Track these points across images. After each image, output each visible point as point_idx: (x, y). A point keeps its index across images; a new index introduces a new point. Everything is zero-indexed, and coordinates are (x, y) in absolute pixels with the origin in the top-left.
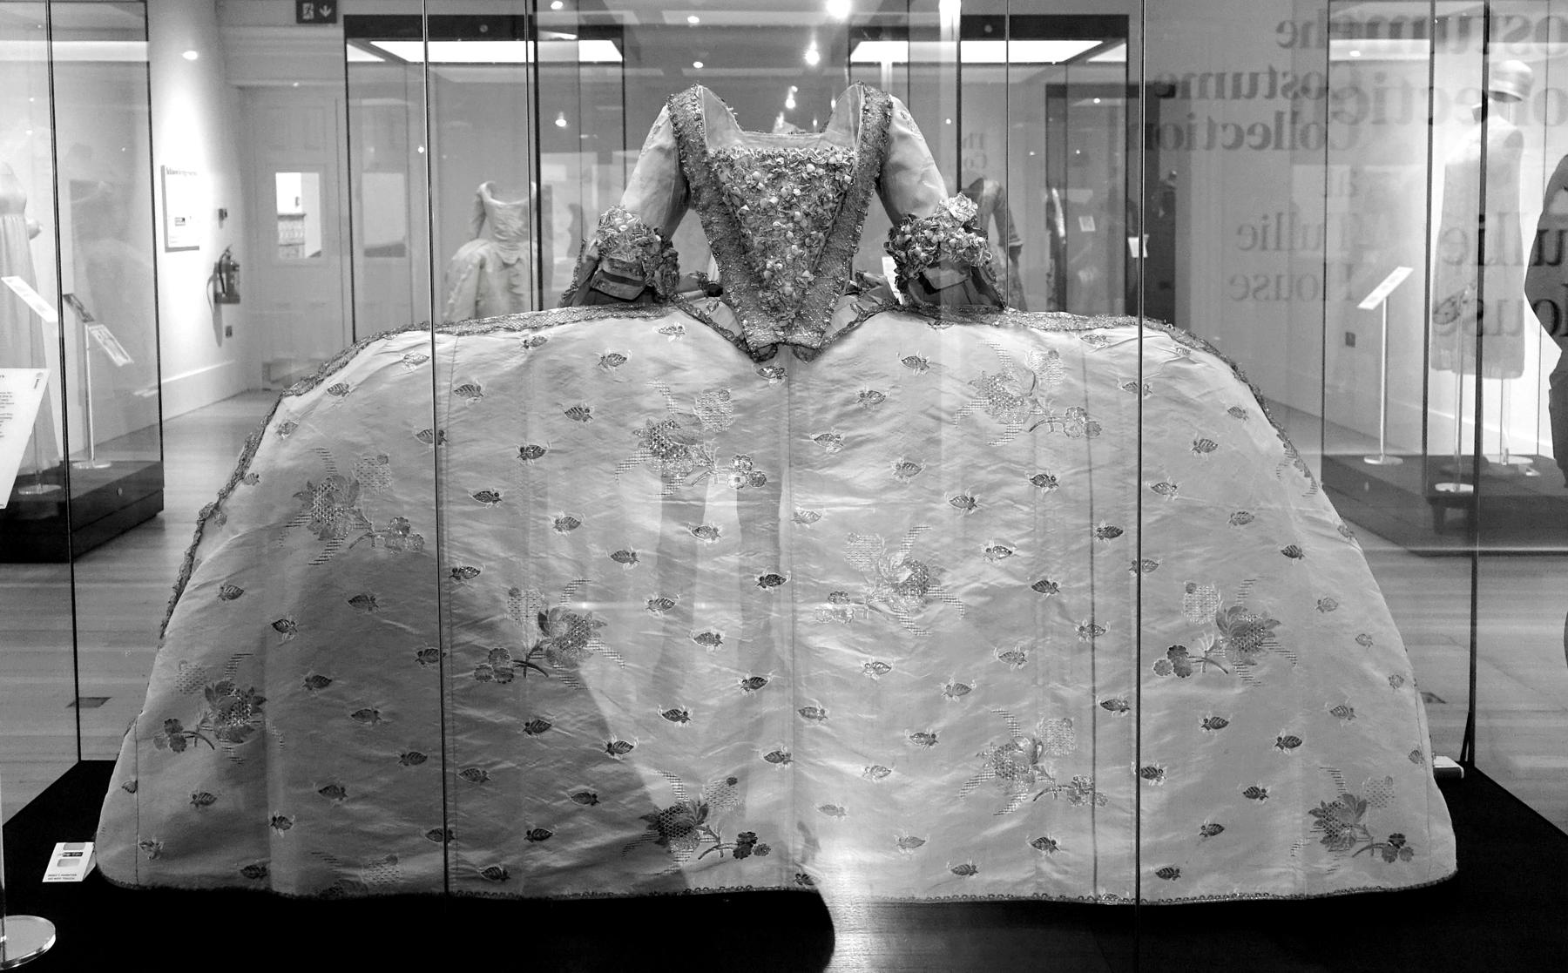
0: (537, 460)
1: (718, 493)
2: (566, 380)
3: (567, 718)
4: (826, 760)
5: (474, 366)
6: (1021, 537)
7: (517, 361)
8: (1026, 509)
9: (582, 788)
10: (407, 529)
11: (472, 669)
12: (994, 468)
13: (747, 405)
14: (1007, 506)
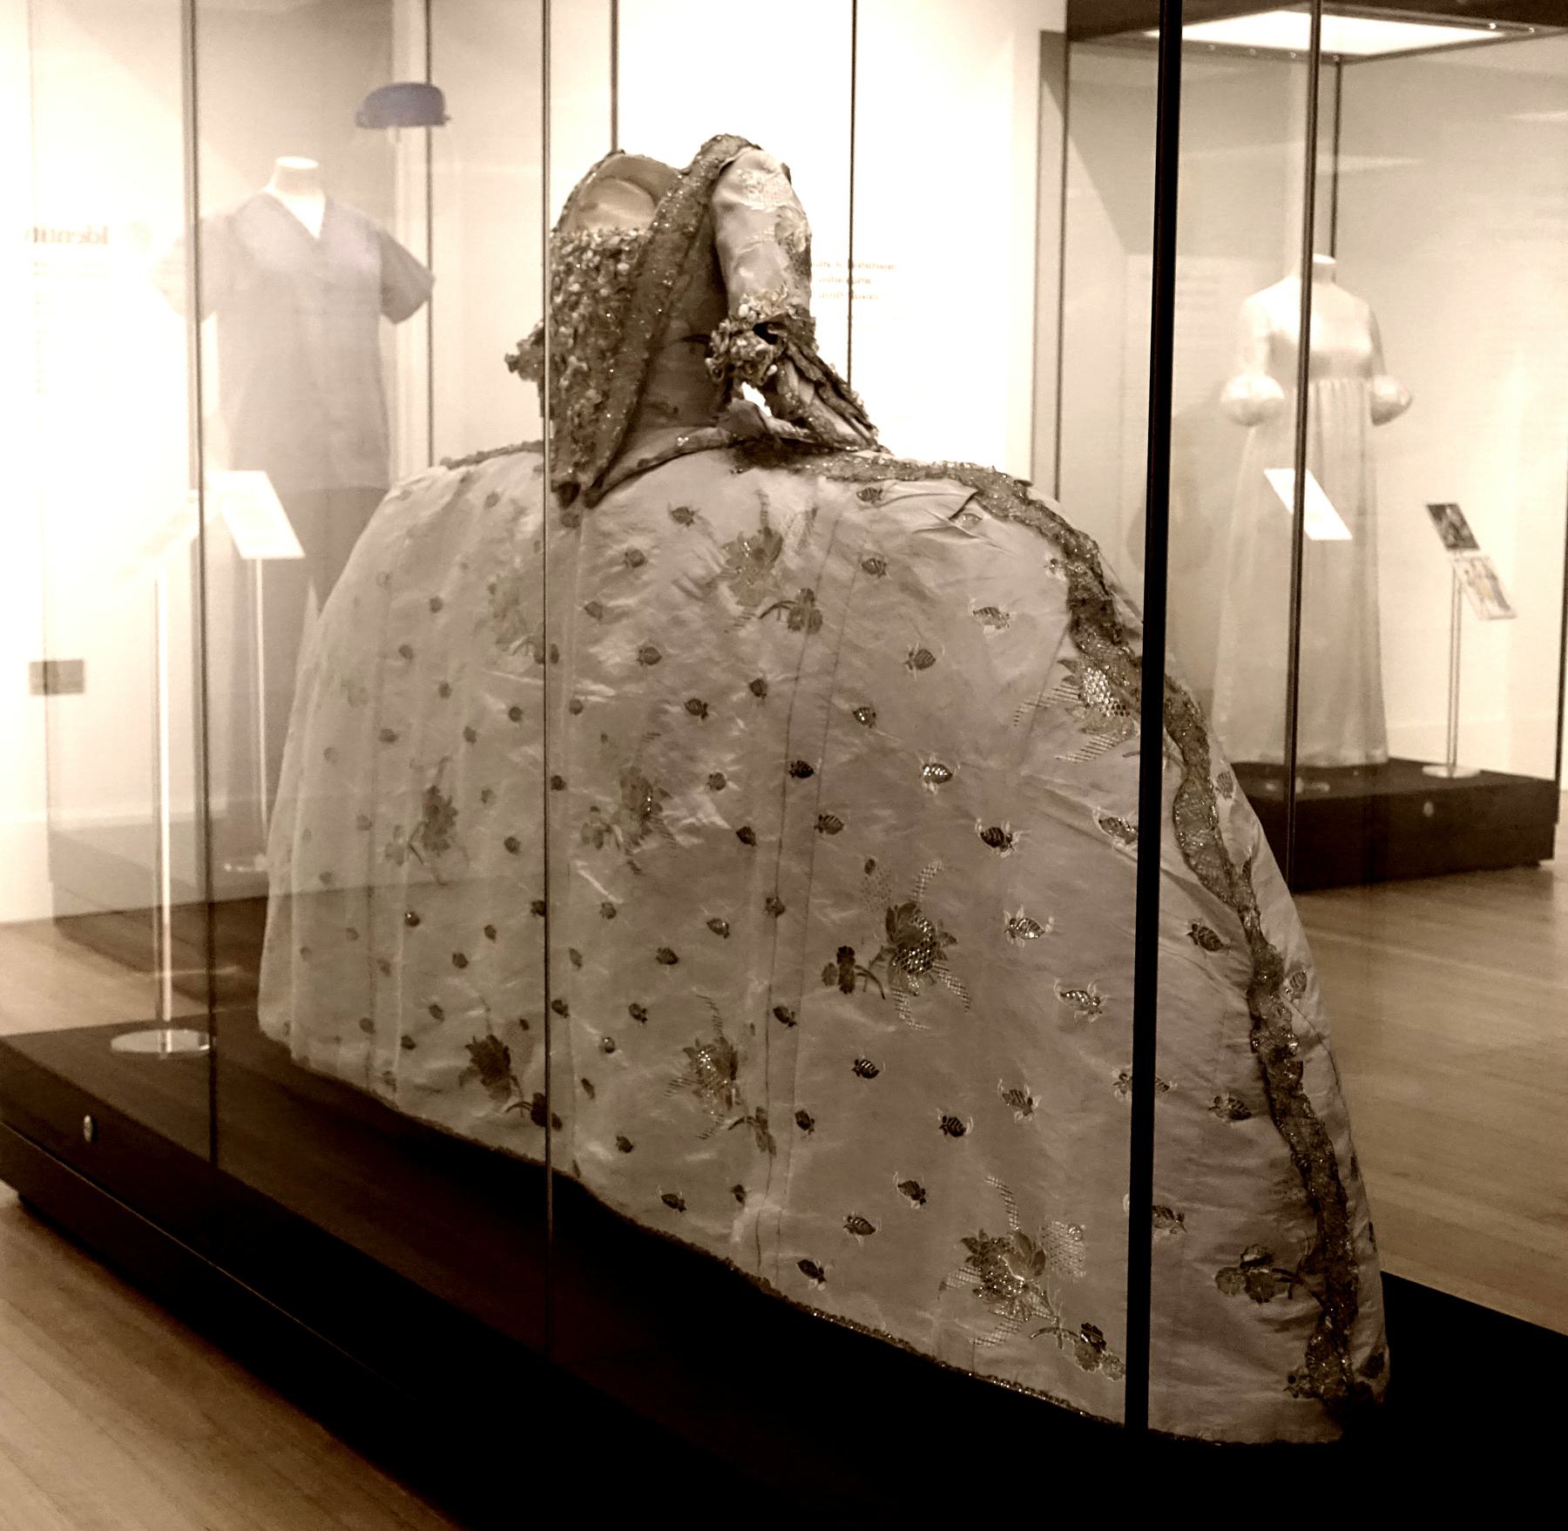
7: (447, 499)
9: (435, 999)
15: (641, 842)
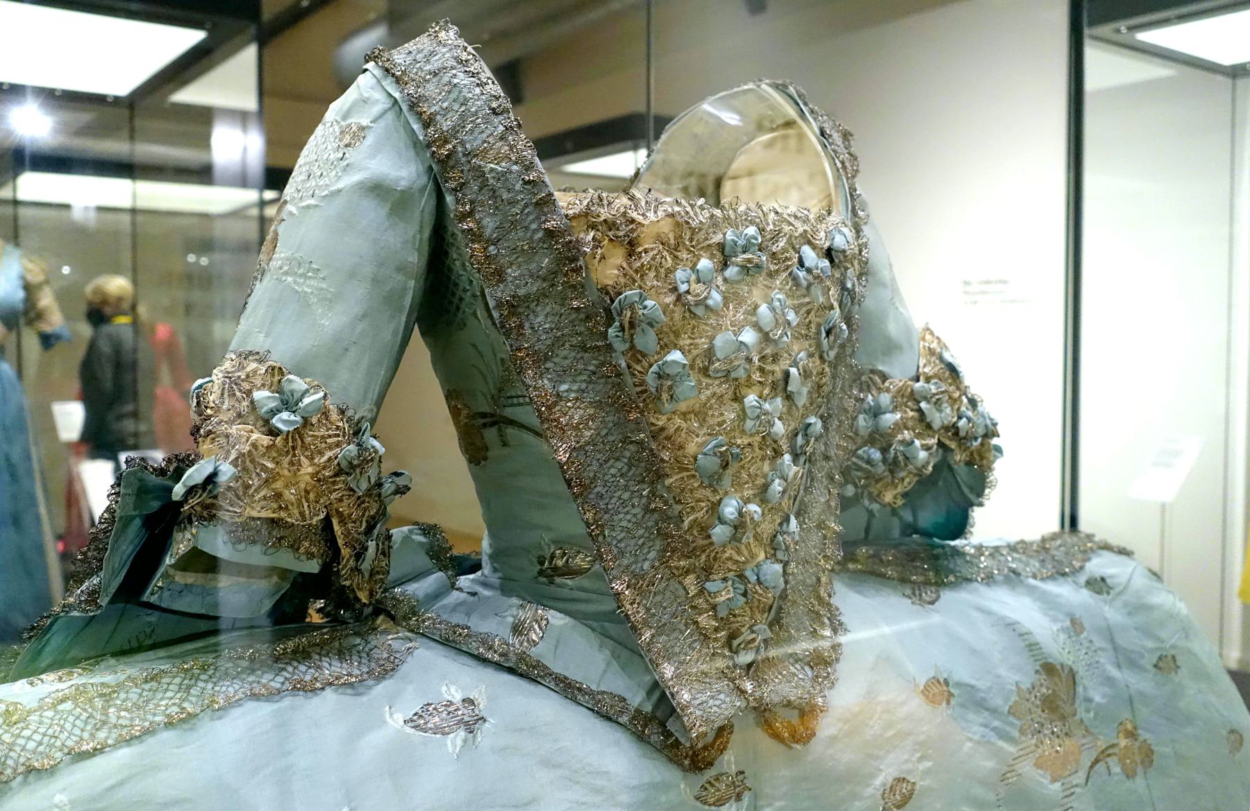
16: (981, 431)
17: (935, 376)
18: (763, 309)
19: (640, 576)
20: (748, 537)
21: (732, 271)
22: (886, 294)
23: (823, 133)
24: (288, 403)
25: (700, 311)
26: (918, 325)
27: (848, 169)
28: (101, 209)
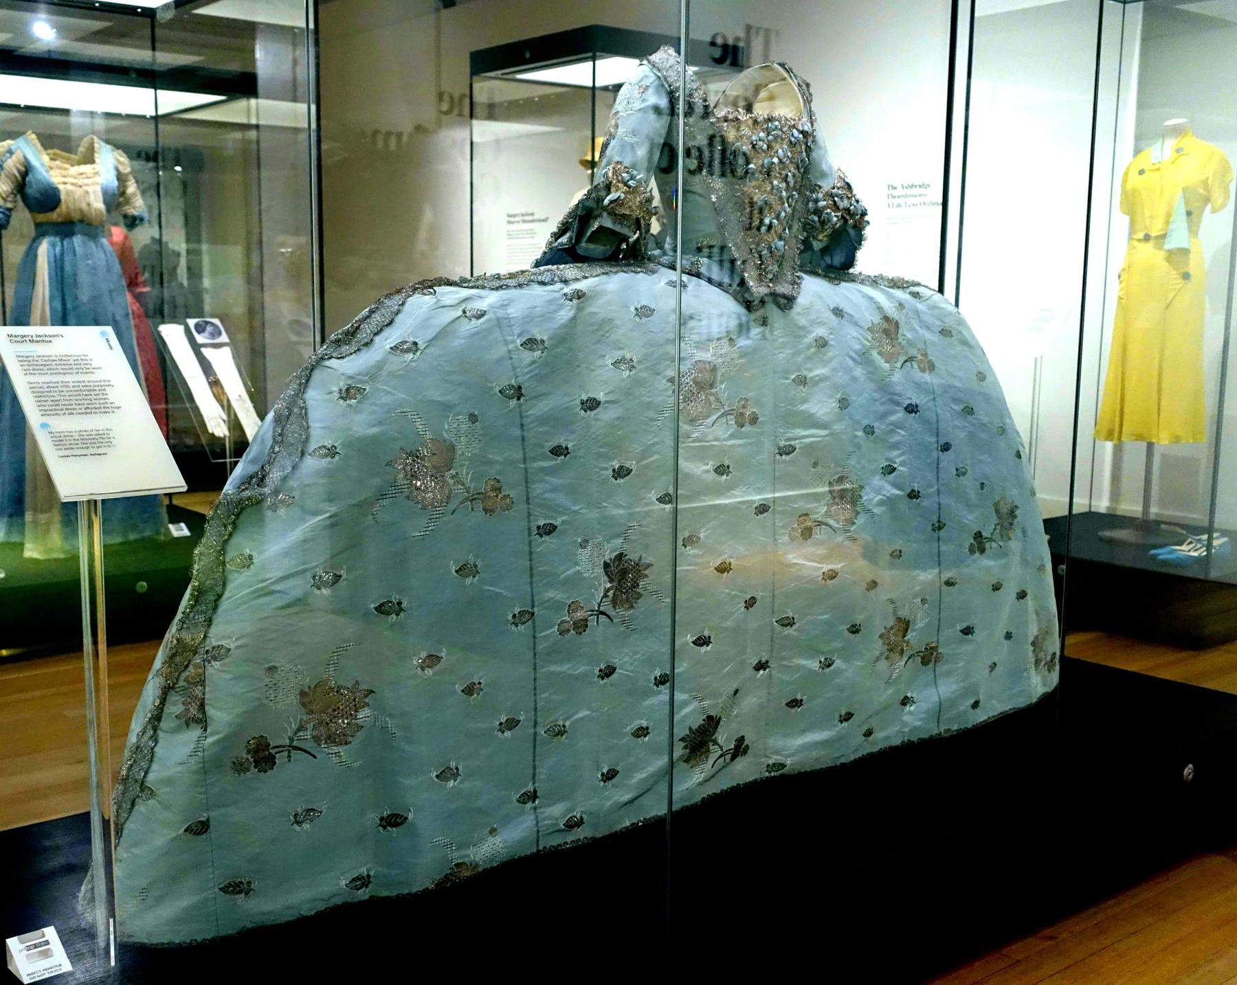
0: (595, 411)
1: (729, 433)
2: (607, 331)
3: (627, 659)
4: (794, 660)
5: (529, 319)
6: (900, 456)
8: (902, 432)
10: (499, 490)
11: (554, 625)
12: (883, 400)
13: (749, 350)
14: (892, 431)
15: (855, 521)
16: (860, 212)
17: (842, 187)
18: (780, 151)
19: (737, 244)
20: (773, 231)
21: (770, 137)
22: (822, 152)
23: (799, 85)
24: (632, 178)
25: (760, 151)
26: (835, 167)
27: (808, 100)
28: (109, 115)
